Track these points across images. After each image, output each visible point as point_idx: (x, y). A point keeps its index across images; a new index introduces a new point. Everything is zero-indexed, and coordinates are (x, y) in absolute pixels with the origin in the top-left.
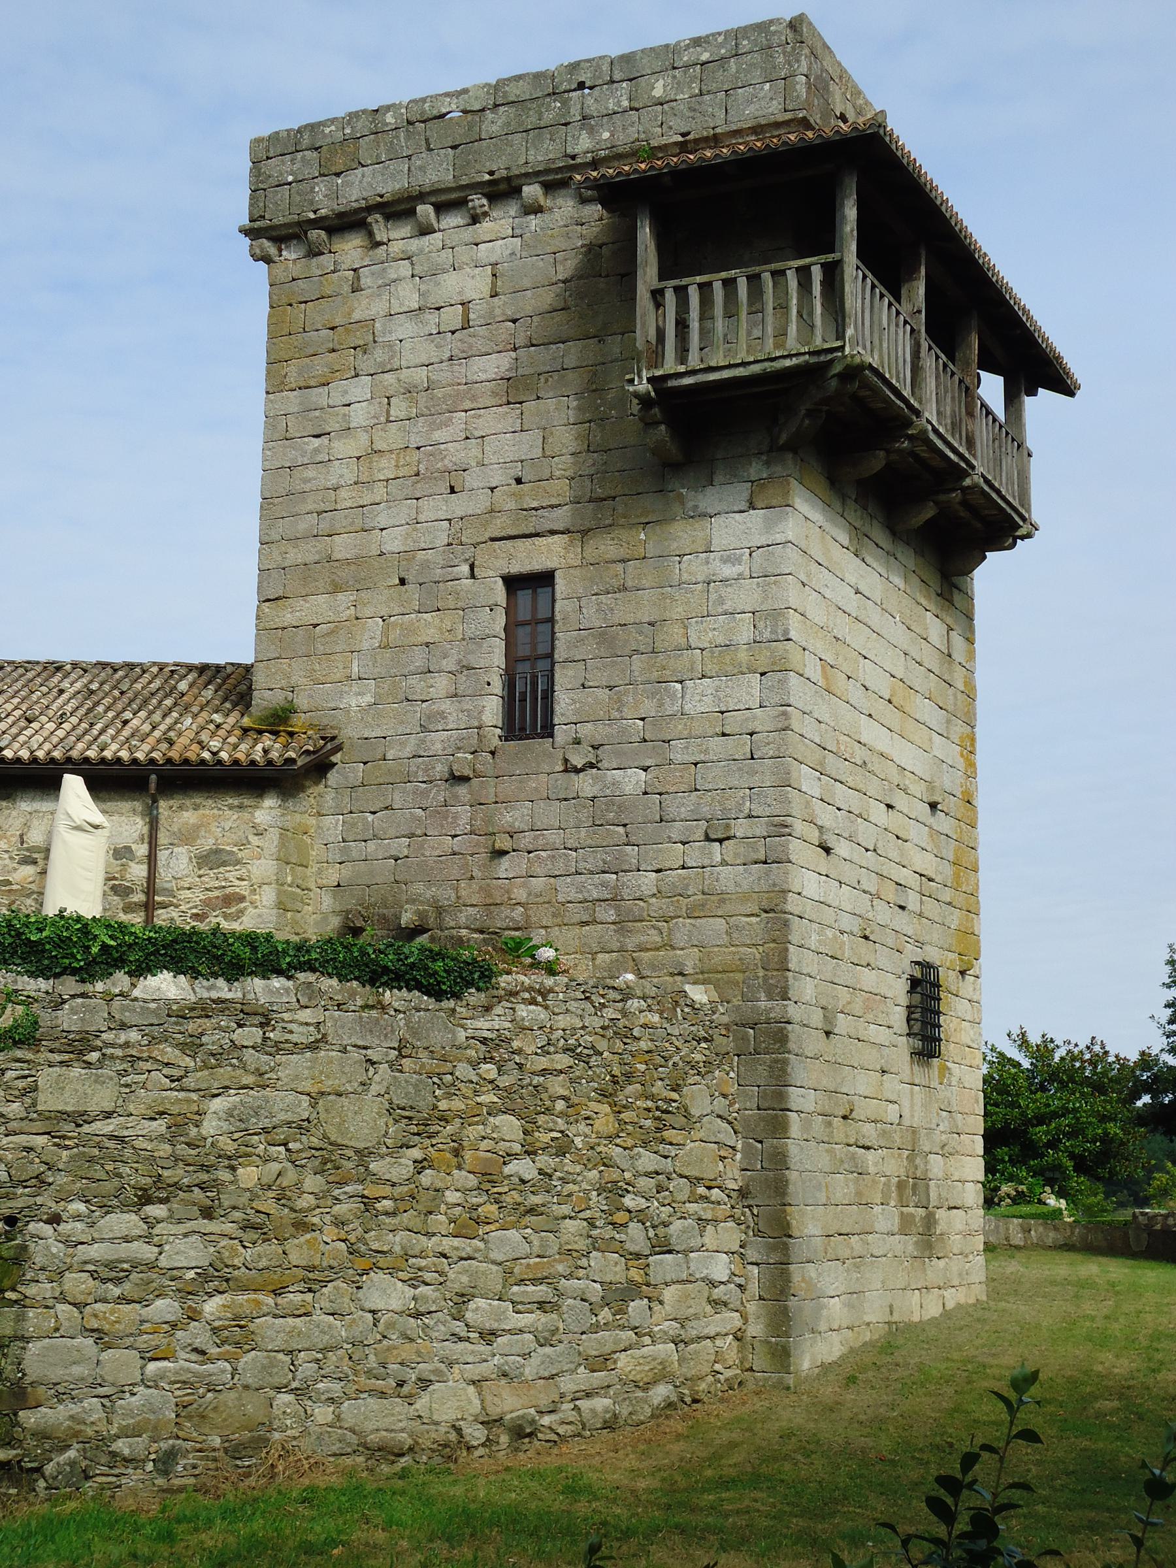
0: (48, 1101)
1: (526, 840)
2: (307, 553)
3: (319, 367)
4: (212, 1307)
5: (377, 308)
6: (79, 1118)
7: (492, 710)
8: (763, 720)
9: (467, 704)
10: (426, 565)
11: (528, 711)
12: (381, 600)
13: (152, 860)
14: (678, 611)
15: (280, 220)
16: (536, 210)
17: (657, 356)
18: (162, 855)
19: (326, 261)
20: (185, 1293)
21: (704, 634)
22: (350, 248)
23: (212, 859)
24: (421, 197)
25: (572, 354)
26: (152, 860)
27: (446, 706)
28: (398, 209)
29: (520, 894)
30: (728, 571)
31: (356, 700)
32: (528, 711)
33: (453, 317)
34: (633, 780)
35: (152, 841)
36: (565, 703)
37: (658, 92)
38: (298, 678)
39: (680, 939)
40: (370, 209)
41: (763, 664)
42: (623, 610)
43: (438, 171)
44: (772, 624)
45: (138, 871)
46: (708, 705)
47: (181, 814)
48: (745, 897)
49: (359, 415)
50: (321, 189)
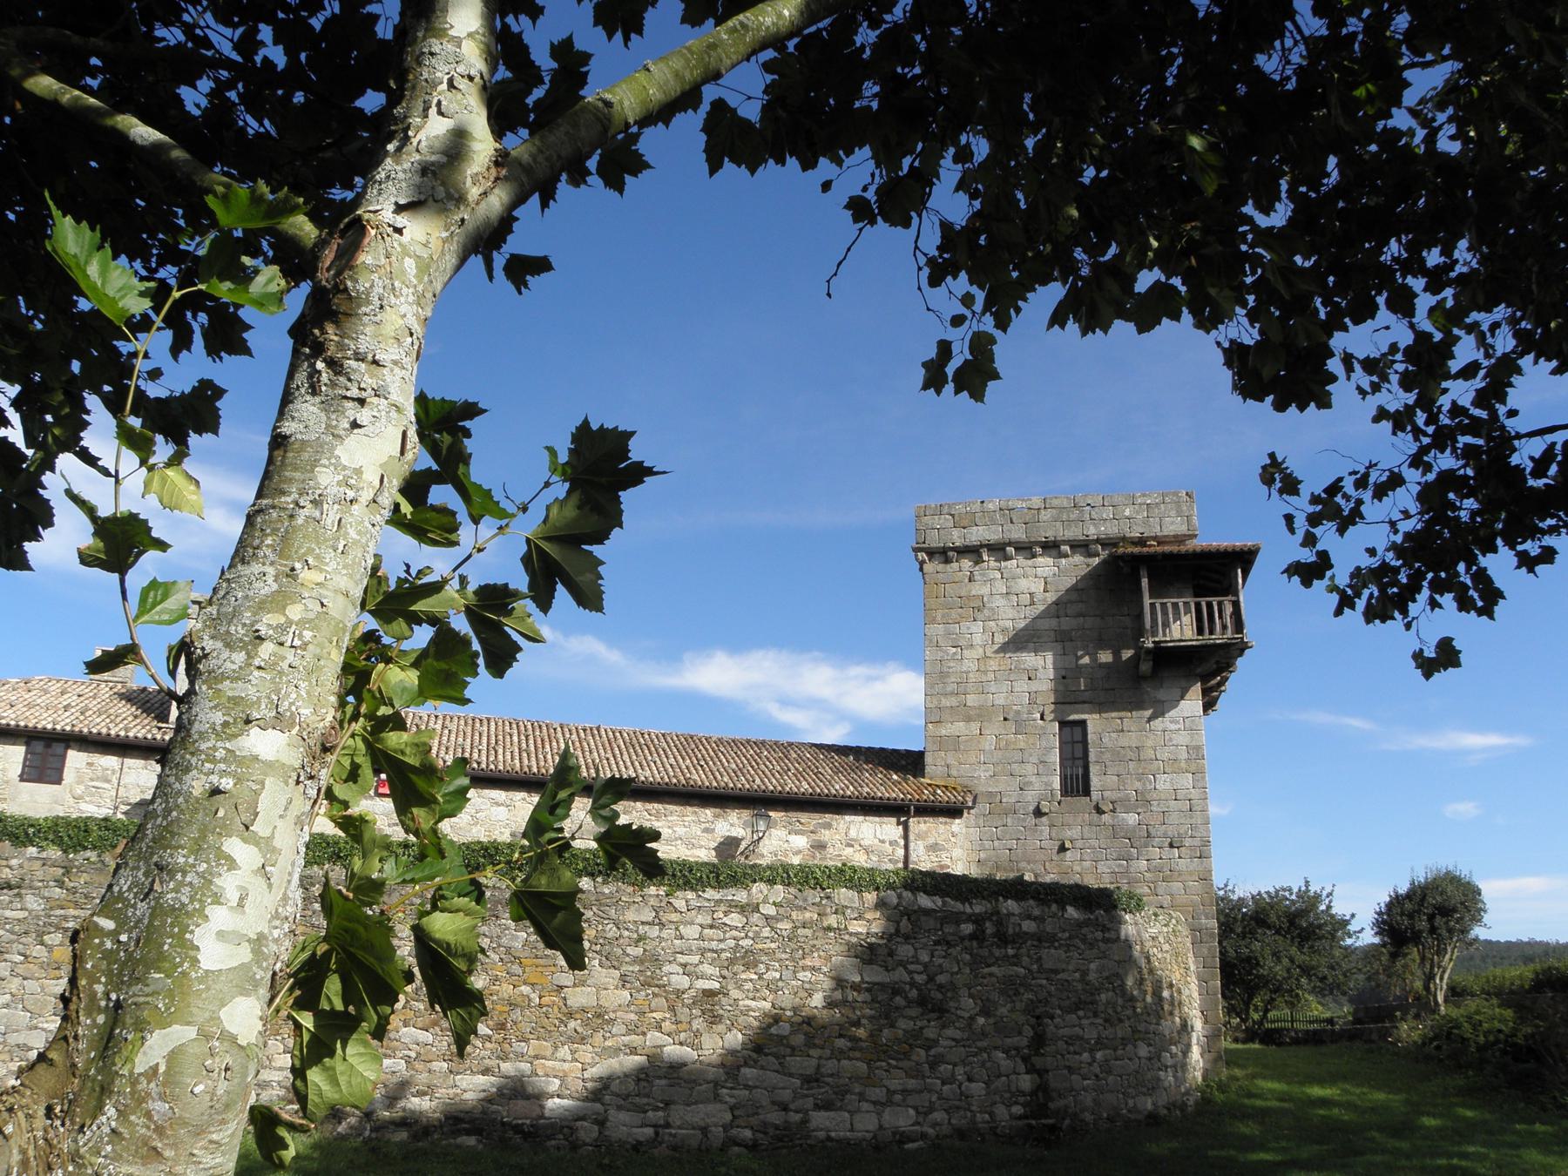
0: (1048, 965)
1: (1079, 844)
2: (951, 701)
3: (954, 614)
4: (1099, 1055)
5: (985, 590)
6: (1056, 972)
7: (1056, 783)
8: (1194, 794)
9: (1045, 779)
10: (1018, 712)
11: (1076, 783)
12: (994, 728)
13: (906, 847)
14: (1149, 743)
15: (934, 545)
16: (1066, 556)
17: (1154, 634)
18: (912, 846)
19: (955, 565)
20: (1091, 1051)
21: (1164, 754)
22: (966, 563)
23: (934, 848)
24: (1010, 544)
25: (1089, 622)
26: (906, 847)
27: (1033, 779)
28: (999, 549)
29: (1077, 868)
30: (1173, 727)
31: (983, 773)
32: (1076, 783)
33: (1026, 599)
34: (1132, 819)
35: (906, 837)
36: (1095, 781)
37: (1127, 513)
38: (951, 761)
39: (1160, 891)
40: (982, 546)
41: (1193, 769)
42: (1125, 741)
43: (1018, 533)
44: (1195, 752)
45: (901, 852)
46: (1168, 786)
47: (918, 825)
48: (1191, 873)
49: (978, 639)
50: (956, 533)
